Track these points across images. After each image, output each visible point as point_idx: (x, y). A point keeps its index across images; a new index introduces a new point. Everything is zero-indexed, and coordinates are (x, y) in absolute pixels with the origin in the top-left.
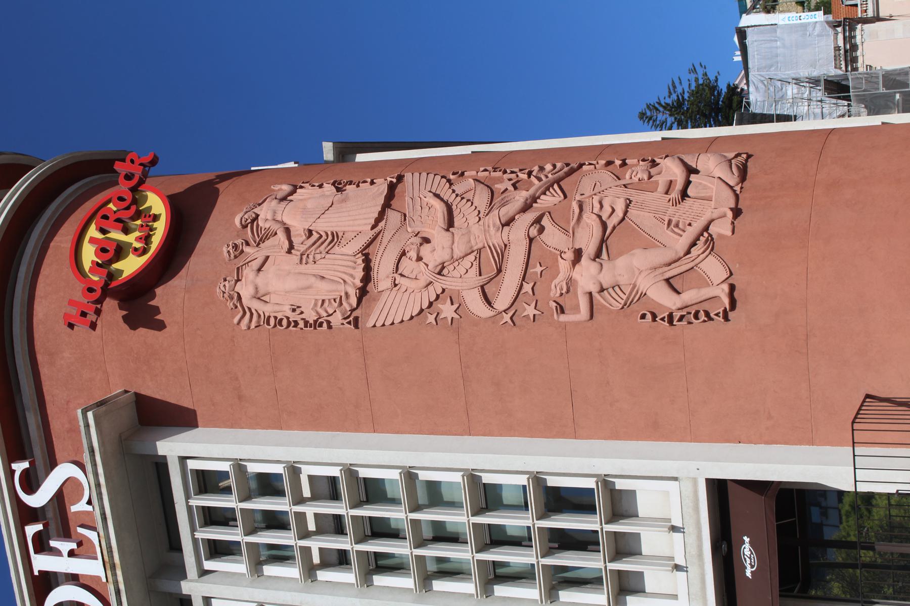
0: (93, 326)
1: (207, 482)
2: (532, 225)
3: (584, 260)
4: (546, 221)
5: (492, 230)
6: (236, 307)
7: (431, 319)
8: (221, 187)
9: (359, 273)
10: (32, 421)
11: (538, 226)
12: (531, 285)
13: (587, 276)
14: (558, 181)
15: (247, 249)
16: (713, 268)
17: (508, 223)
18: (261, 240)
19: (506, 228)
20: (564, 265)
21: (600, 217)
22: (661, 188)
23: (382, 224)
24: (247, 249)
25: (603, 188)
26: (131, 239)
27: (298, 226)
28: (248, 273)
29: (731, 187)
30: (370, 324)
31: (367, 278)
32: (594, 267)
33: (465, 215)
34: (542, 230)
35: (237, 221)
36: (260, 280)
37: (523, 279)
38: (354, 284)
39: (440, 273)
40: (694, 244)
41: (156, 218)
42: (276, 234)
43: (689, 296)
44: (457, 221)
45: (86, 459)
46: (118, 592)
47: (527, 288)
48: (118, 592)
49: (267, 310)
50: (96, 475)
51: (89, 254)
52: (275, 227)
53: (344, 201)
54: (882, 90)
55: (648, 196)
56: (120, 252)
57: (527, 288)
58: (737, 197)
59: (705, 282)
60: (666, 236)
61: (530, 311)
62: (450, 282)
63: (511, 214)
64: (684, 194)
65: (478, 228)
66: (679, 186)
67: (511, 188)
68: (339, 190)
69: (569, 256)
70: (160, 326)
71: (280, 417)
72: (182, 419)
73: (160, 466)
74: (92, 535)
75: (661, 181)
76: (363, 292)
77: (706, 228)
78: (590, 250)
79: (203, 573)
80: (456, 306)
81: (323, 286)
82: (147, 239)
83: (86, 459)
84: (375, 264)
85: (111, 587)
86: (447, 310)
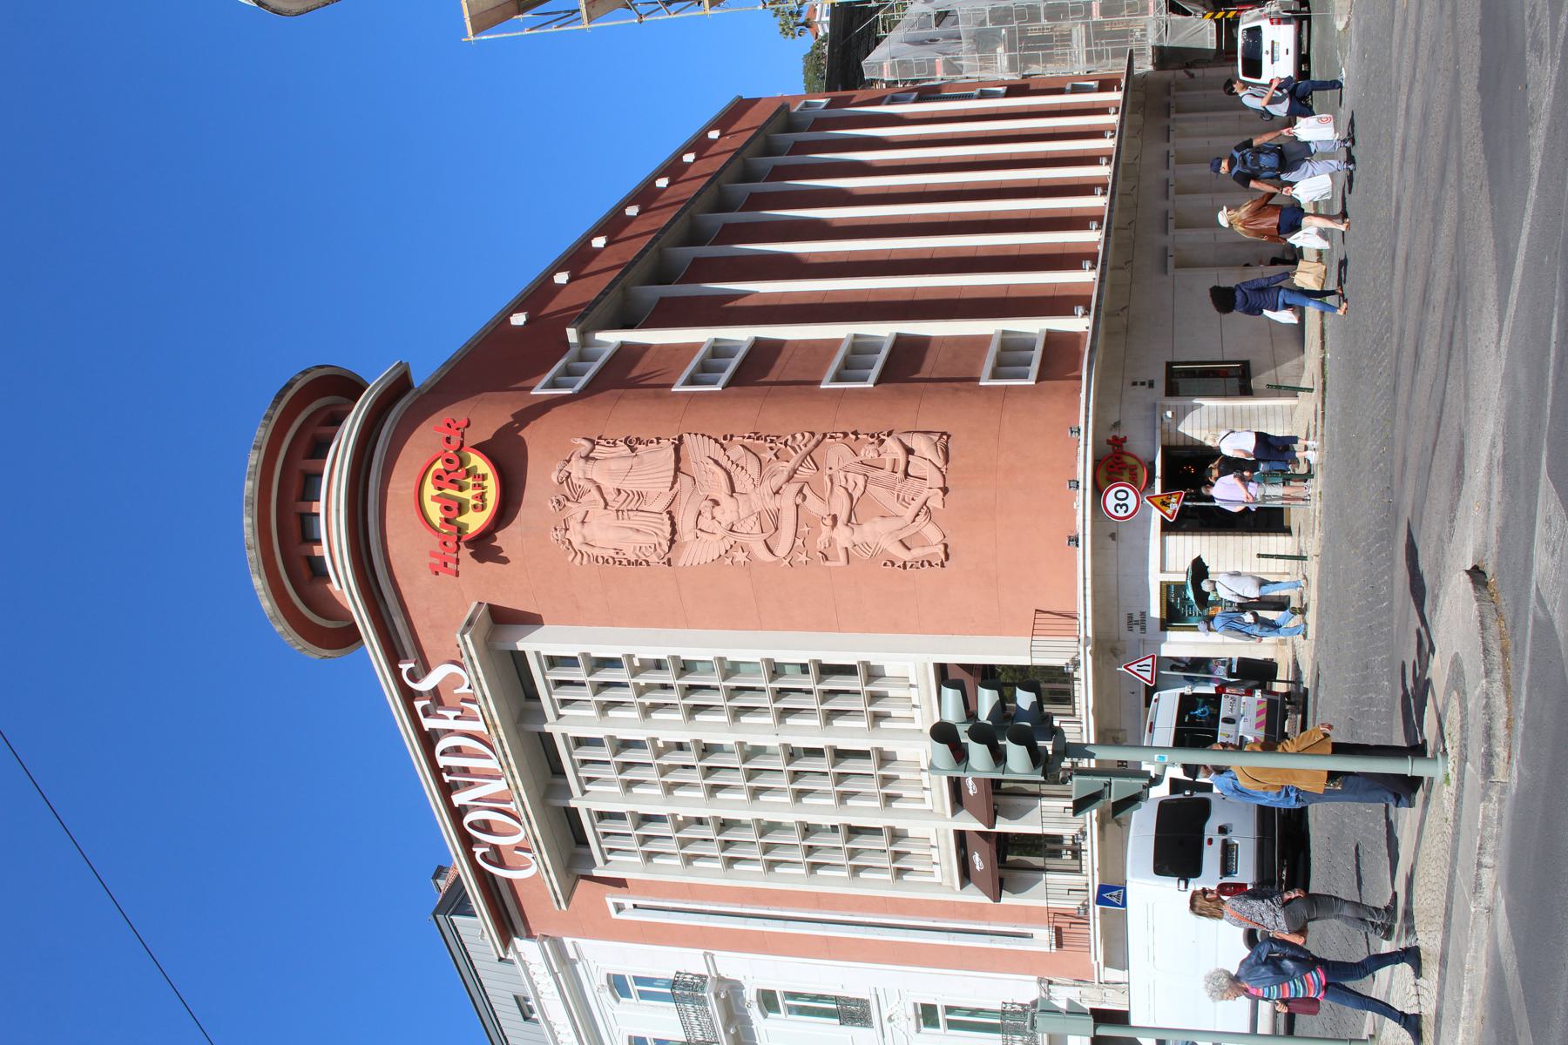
0: (457, 574)
1: (553, 662)
3: (839, 523)
4: (806, 490)
7: (728, 561)
8: (524, 433)
9: (668, 529)
10: (399, 622)
13: (842, 536)
15: (569, 504)
16: (932, 533)
20: (826, 530)
22: (888, 466)
23: (677, 486)
26: (468, 494)
27: (609, 486)
28: (574, 525)
30: (681, 564)
31: (674, 532)
32: (847, 531)
34: (805, 498)
35: (554, 479)
36: (586, 530)
41: (484, 477)
43: (917, 553)
45: (465, 660)
46: (500, 741)
47: (799, 542)
48: (500, 741)
49: (596, 552)
50: (475, 672)
51: (435, 512)
52: (588, 486)
53: (641, 463)
54: (989, 25)
55: (879, 473)
56: (461, 508)
57: (799, 542)
61: (803, 558)
62: (741, 539)
64: (906, 474)
65: (760, 498)
68: (633, 450)
69: (829, 521)
70: (505, 561)
71: (612, 617)
72: (534, 621)
73: (519, 659)
74: (475, 708)
75: (888, 459)
76: (672, 541)
78: (842, 518)
79: (559, 717)
81: (640, 538)
82: (482, 497)
83: (465, 660)
84: (678, 520)
85: (495, 740)
86: (740, 557)
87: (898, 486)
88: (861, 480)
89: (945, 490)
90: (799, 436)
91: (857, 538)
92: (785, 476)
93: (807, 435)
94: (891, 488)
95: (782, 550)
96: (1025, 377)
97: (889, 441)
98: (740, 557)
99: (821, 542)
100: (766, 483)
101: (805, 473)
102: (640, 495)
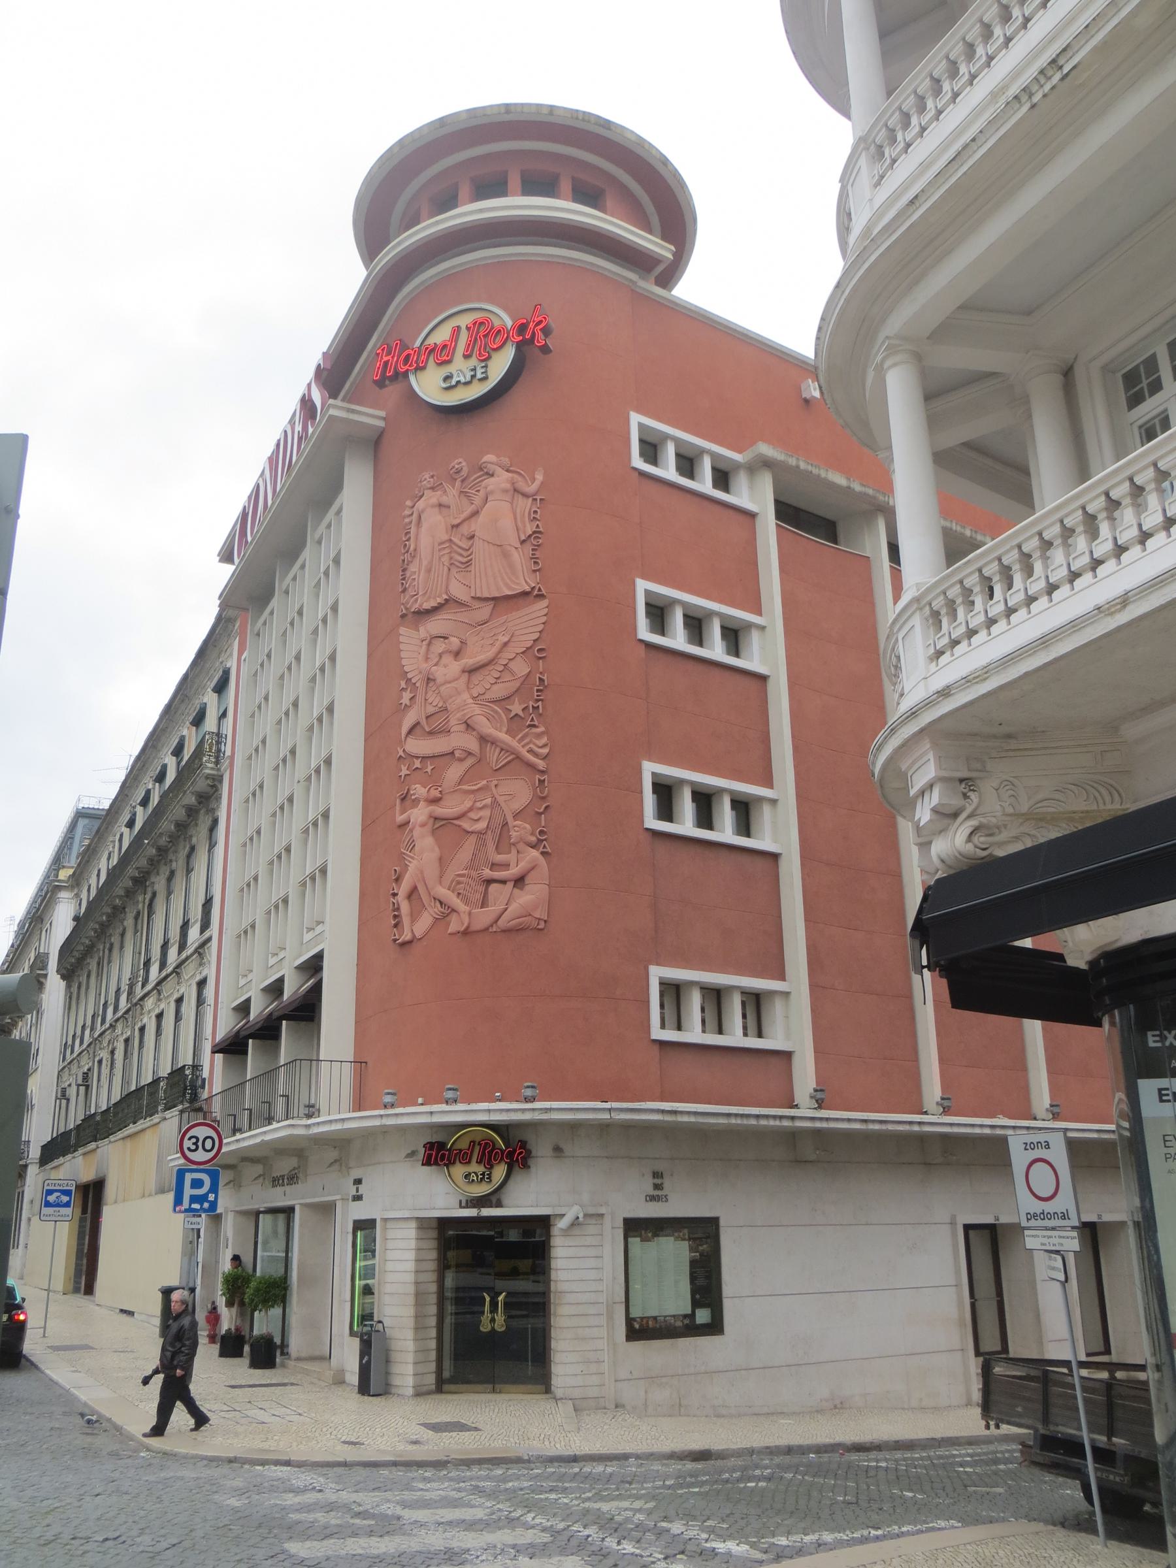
3: (432, 808)
4: (470, 761)
5: (458, 715)
11: (463, 756)
13: (419, 814)
14: (518, 757)
15: (458, 483)
17: (468, 727)
19: (463, 727)
21: (471, 809)
22: (500, 858)
23: (477, 604)
24: (458, 483)
25: (503, 804)
27: (476, 526)
29: (496, 921)
33: (483, 681)
34: (461, 760)
44: (476, 678)
47: (417, 764)
49: (413, 530)
52: (478, 500)
55: (491, 847)
58: (487, 929)
59: (414, 918)
60: (450, 875)
61: (404, 771)
63: (476, 727)
66: (497, 875)
69: (435, 793)
77: (453, 910)
87: (474, 874)
88: (482, 825)
89: (466, 933)
90: (544, 740)
91: (417, 832)
92: (488, 729)
93: (545, 751)
94: (472, 865)
96: (663, 1026)
97: (535, 853)
98: (406, 698)
99: (419, 791)
100: (477, 710)
101: (493, 755)
102: (468, 563)
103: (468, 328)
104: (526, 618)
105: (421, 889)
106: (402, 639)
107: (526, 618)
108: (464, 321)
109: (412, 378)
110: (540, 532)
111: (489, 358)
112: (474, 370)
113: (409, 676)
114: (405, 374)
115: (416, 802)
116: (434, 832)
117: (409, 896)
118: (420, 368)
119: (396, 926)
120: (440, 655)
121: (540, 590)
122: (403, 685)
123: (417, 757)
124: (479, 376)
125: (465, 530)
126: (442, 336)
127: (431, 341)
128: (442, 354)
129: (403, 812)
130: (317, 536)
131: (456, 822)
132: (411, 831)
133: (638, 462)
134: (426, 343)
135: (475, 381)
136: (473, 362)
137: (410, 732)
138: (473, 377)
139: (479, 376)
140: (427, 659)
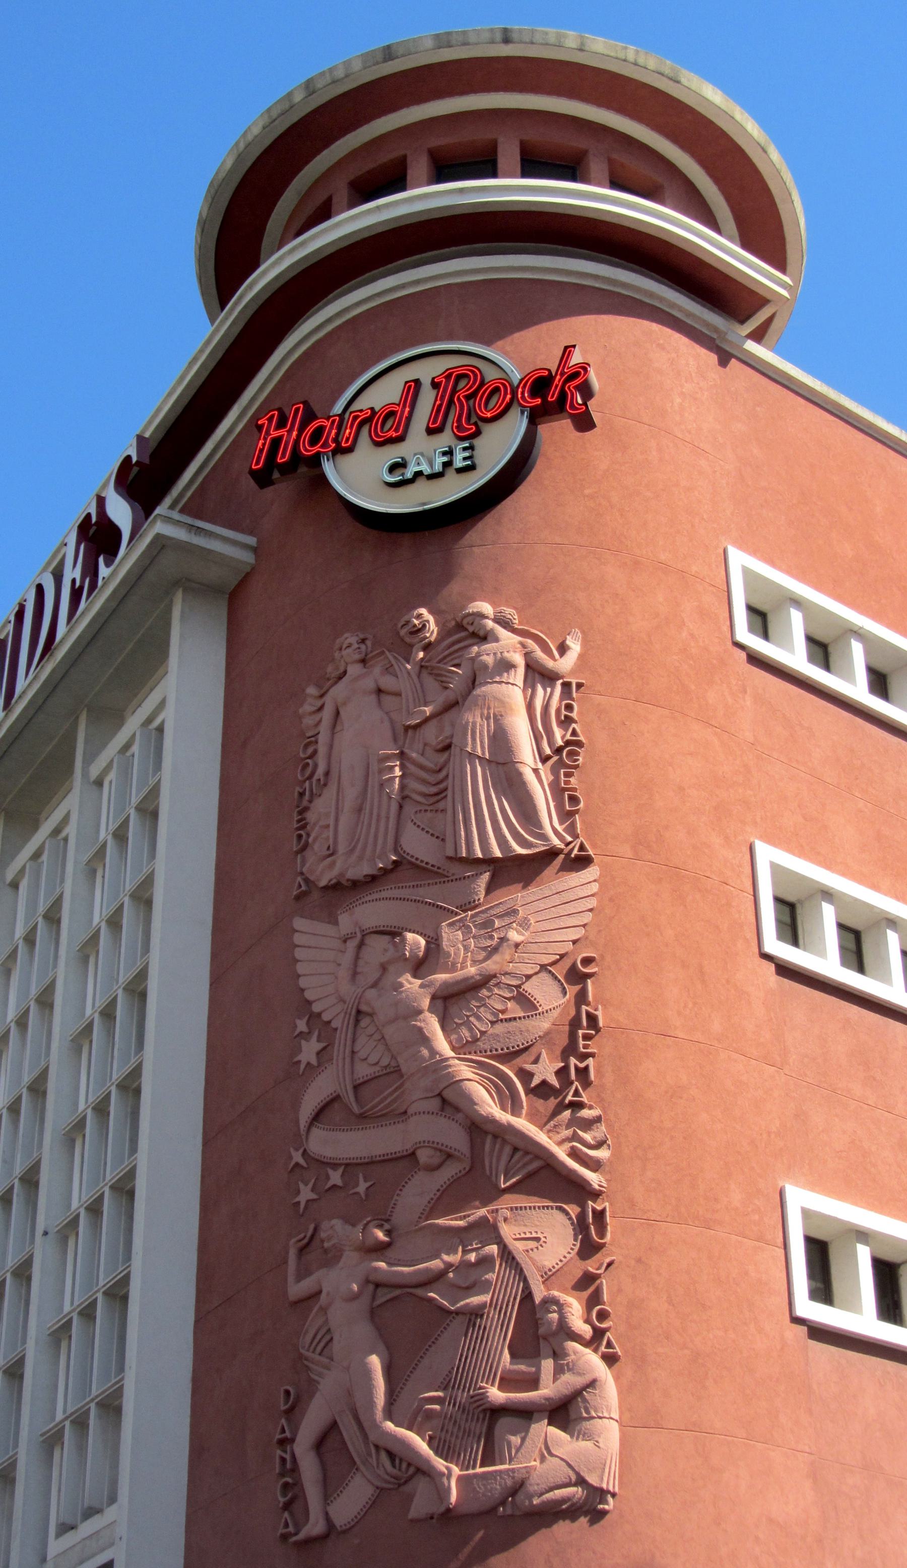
2: (436, 1149)
4: (450, 1171)
6: (329, 679)
11: (436, 1161)
12: (339, 1182)
18: (433, 668)
19: (435, 1103)
34: (432, 1169)
37: (347, 1165)
38: (348, 868)
39: (359, 1012)
40: (391, 1455)
42: (446, 688)
47: (336, 1178)
49: (323, 738)
61: (306, 1194)
67: (536, 1081)
80: (314, 1062)
91: (338, 1314)
95: (324, 1143)
98: (309, 1051)
103: (435, 385)
104: (557, 900)
105: (348, 1430)
106: (298, 939)
107: (557, 900)
108: (427, 371)
109: (328, 468)
110: (579, 744)
111: (478, 433)
112: (450, 453)
113: (316, 1008)
114: (315, 462)
115: (331, 1257)
116: (373, 1314)
117: (319, 1445)
118: (342, 450)
119: (287, 1506)
120: (384, 968)
121: (582, 848)
122: (302, 1025)
123: (335, 1166)
124: (459, 462)
125: (431, 734)
126: (385, 394)
127: (363, 403)
128: (388, 427)
129: (303, 1273)
130: (95, 771)
131: (419, 1292)
132: (324, 1310)
133: (744, 635)
134: (356, 406)
135: (450, 474)
136: (446, 439)
137: (317, 1117)
138: (447, 465)
139: (459, 462)
140: (355, 974)
